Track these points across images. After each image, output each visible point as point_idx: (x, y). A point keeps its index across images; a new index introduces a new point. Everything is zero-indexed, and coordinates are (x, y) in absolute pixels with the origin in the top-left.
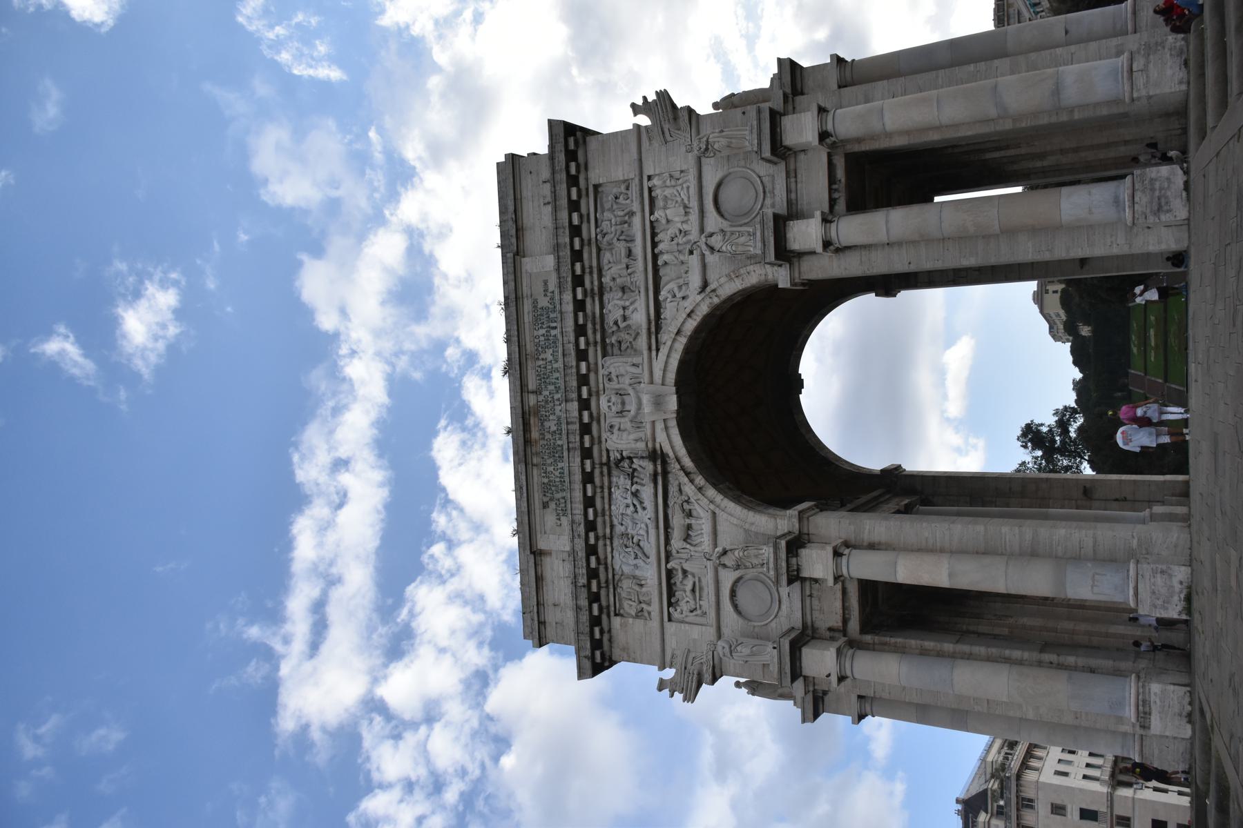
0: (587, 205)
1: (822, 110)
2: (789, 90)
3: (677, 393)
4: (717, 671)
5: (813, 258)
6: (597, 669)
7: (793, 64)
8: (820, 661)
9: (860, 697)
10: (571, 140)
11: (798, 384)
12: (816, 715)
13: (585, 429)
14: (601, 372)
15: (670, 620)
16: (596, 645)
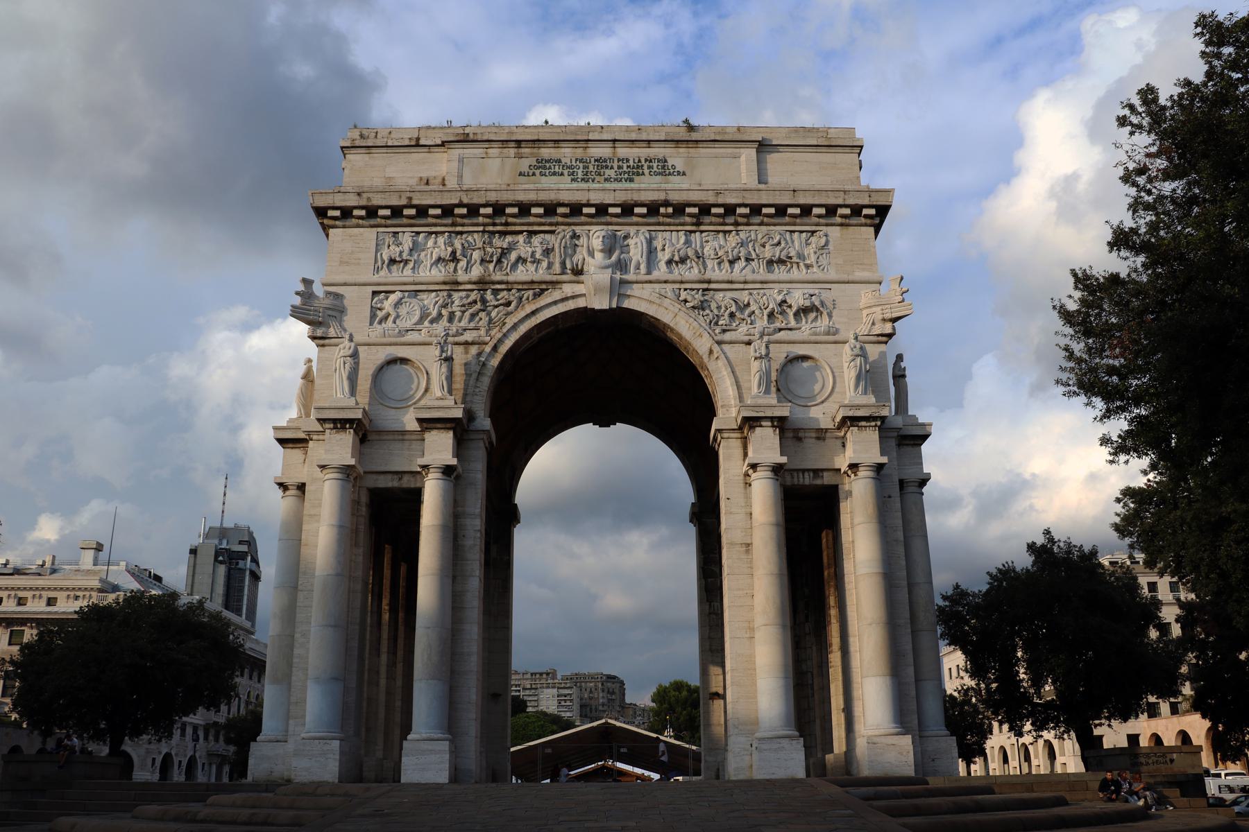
1: (879, 468)
2: (902, 433)
3: (611, 309)
4: (321, 342)
5: (739, 452)
6: (321, 212)
7: (925, 437)
8: (340, 448)
9: (301, 487)
10: (873, 211)
11: (604, 422)
12: (282, 441)
13: (576, 209)
14: (632, 230)
15: (375, 293)
16: (346, 213)
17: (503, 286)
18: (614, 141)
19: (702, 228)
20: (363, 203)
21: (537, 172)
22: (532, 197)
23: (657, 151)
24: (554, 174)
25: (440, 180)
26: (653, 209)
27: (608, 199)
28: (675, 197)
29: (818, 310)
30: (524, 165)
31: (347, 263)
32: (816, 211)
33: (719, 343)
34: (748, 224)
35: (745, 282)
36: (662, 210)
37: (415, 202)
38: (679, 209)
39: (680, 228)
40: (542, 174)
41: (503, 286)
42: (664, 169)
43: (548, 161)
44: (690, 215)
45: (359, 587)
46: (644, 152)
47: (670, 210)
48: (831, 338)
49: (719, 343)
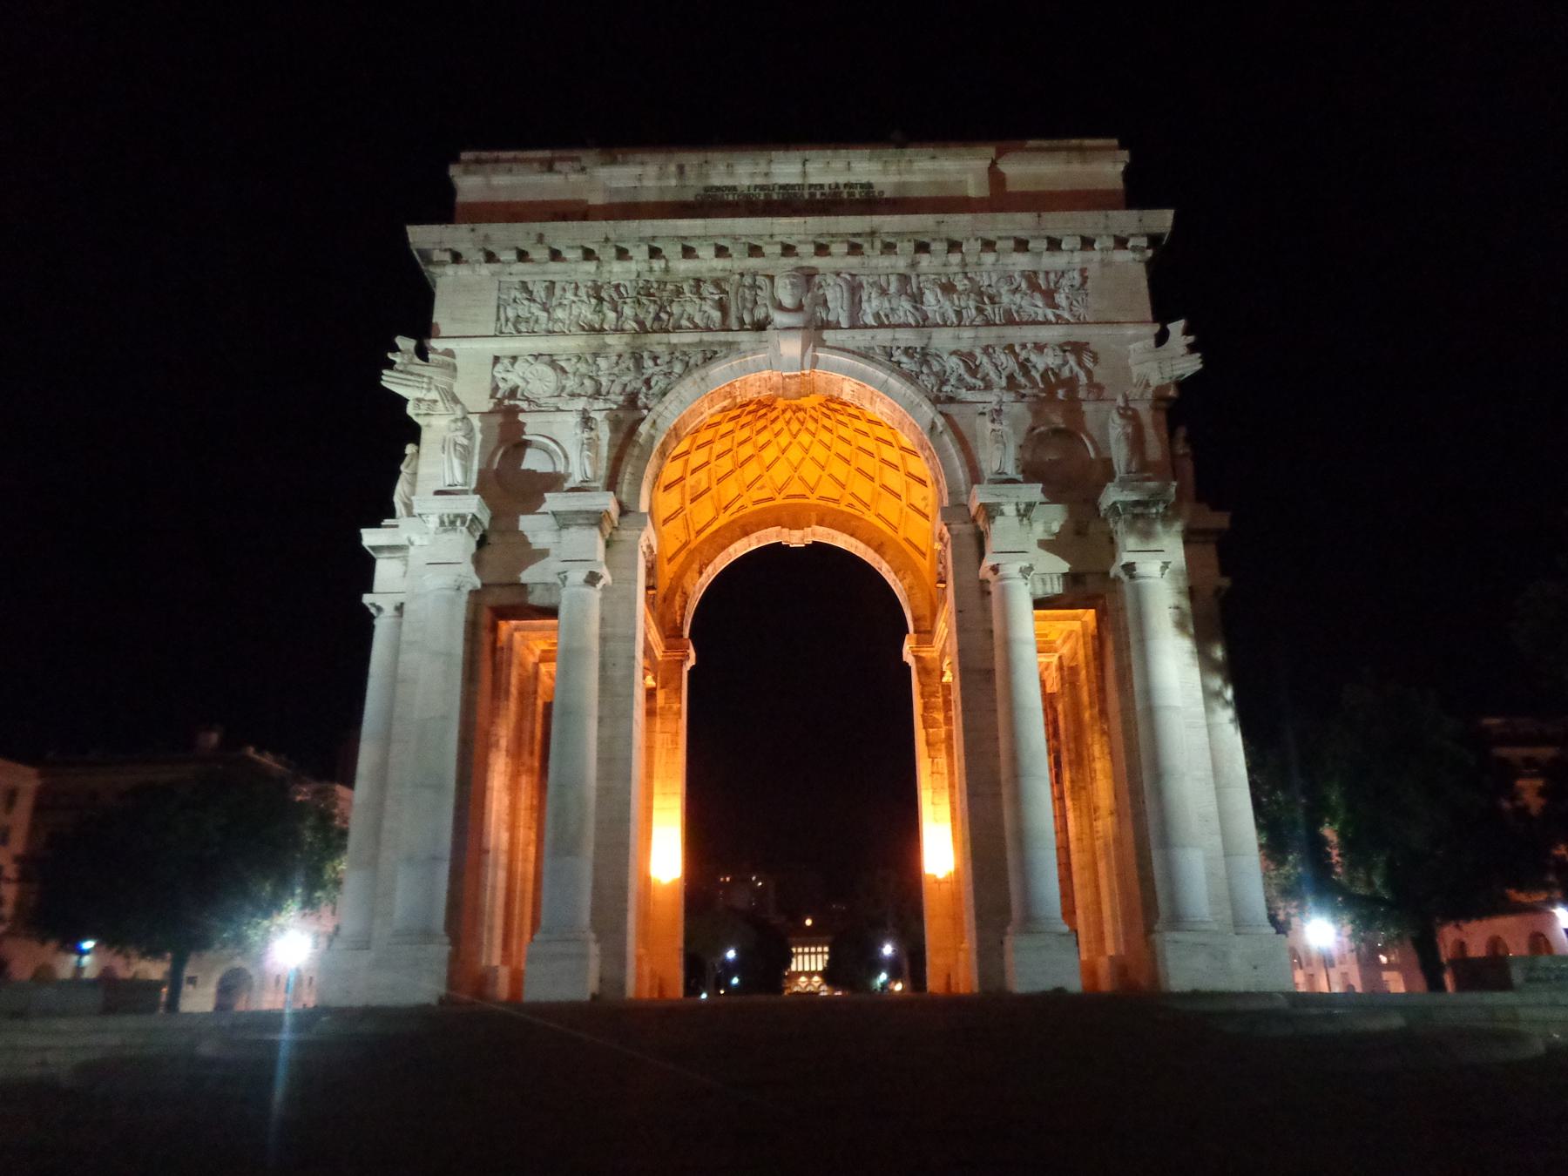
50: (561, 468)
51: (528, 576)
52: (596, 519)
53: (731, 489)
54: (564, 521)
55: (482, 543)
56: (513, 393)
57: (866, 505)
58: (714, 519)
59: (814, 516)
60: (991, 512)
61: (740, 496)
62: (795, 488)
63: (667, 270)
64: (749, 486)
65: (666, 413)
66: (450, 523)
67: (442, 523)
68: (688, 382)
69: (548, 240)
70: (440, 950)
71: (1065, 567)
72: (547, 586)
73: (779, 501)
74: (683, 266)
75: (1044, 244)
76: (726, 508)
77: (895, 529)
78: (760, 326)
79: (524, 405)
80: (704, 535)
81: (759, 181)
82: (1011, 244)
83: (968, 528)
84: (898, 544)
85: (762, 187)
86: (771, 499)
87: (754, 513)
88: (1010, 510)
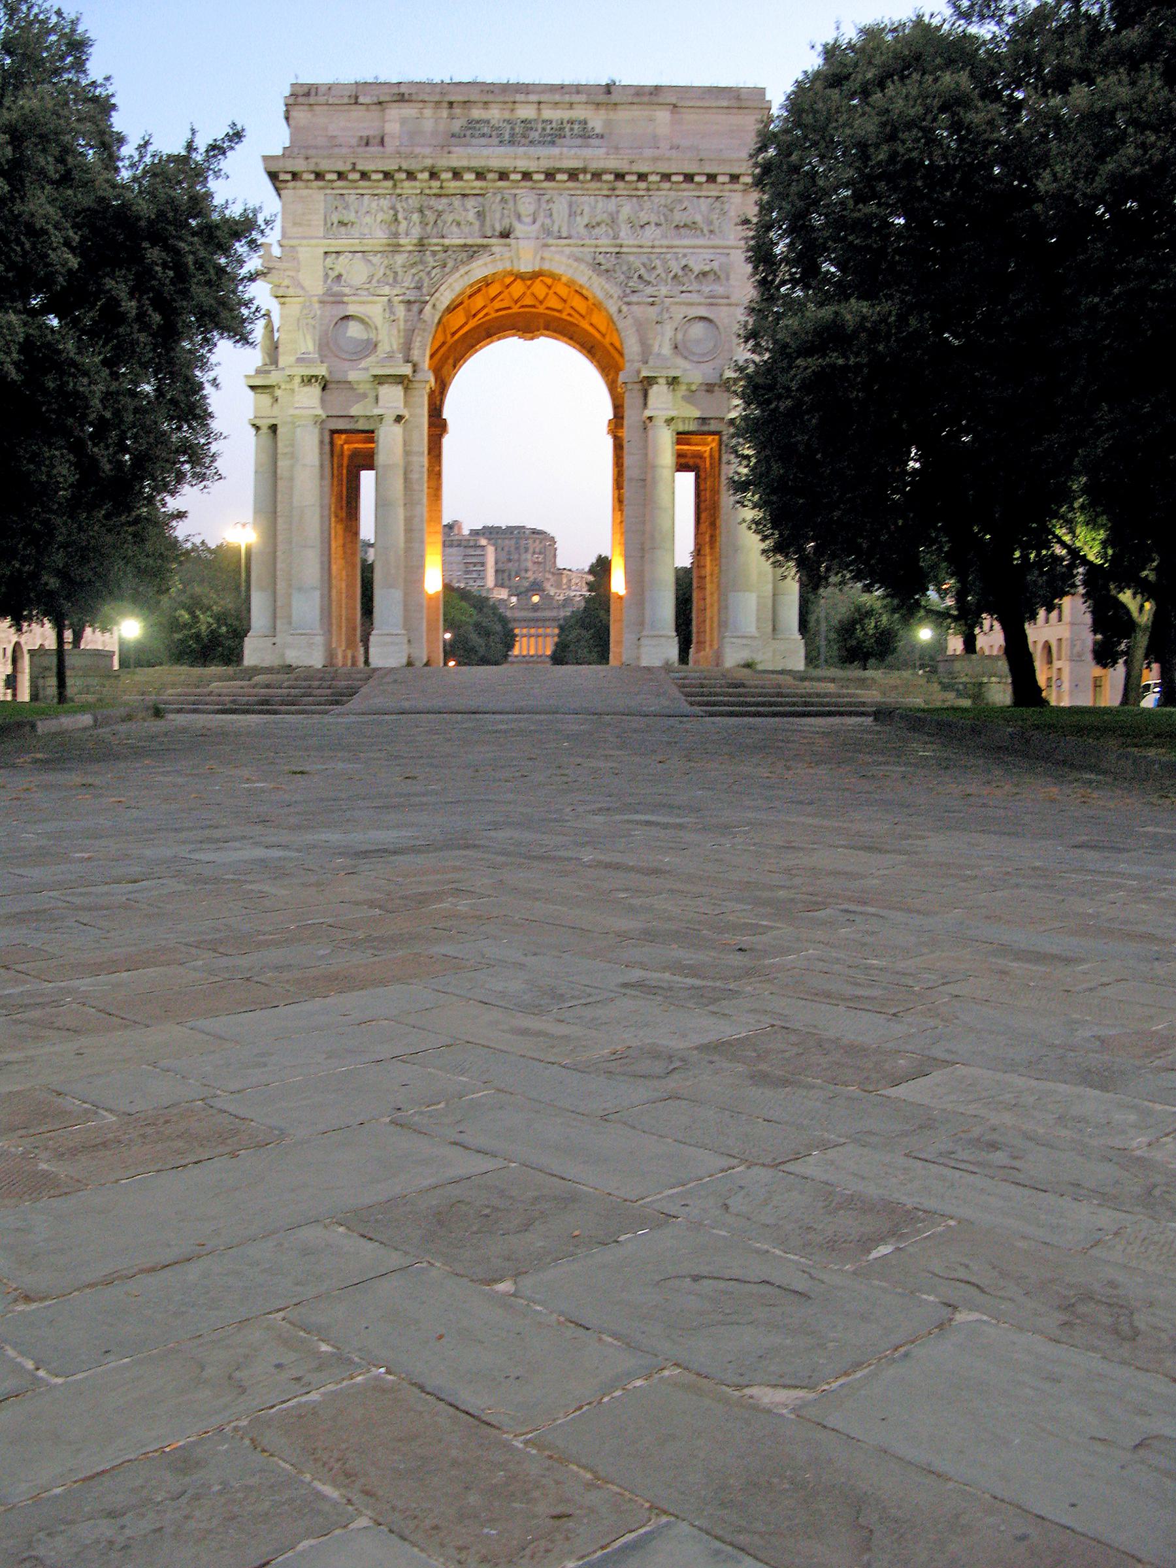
0: (712, 190)
4: (283, 300)
6: (273, 176)
8: (309, 400)
9: (273, 428)
17: (439, 248)
18: (539, 103)
19: (617, 192)
20: (312, 168)
21: (468, 133)
22: (465, 163)
23: (579, 113)
24: (484, 135)
25: (378, 140)
26: (573, 175)
27: (532, 166)
28: (594, 166)
29: (715, 274)
30: (456, 126)
31: (300, 225)
32: (720, 179)
33: (628, 304)
34: (658, 190)
35: (653, 247)
36: (581, 177)
37: (359, 167)
38: (597, 176)
39: (597, 193)
40: (472, 136)
41: (439, 248)
42: (585, 134)
43: (478, 122)
44: (606, 182)
45: (326, 513)
46: (566, 115)
47: (589, 177)
48: (725, 301)
49: (628, 304)
50: (373, 336)
51: (353, 412)
52: (400, 380)
53: (479, 301)
54: (380, 380)
55: (324, 389)
56: (339, 276)
57: (581, 315)
58: (466, 323)
59: (542, 325)
60: (650, 381)
61: (484, 307)
62: (528, 301)
63: (441, 188)
64: (493, 299)
65: (442, 298)
66: (308, 380)
67: (303, 381)
68: (457, 275)
69: (359, 167)
70: (319, 640)
71: (697, 414)
72: (368, 417)
73: (515, 310)
74: (453, 186)
75: (704, 179)
76: (474, 316)
77: (604, 336)
78: (505, 235)
79: (347, 290)
80: (456, 337)
81: (507, 115)
82: (681, 178)
83: (638, 386)
84: (604, 346)
85: (509, 122)
86: (509, 308)
87: (496, 318)
88: (662, 381)
